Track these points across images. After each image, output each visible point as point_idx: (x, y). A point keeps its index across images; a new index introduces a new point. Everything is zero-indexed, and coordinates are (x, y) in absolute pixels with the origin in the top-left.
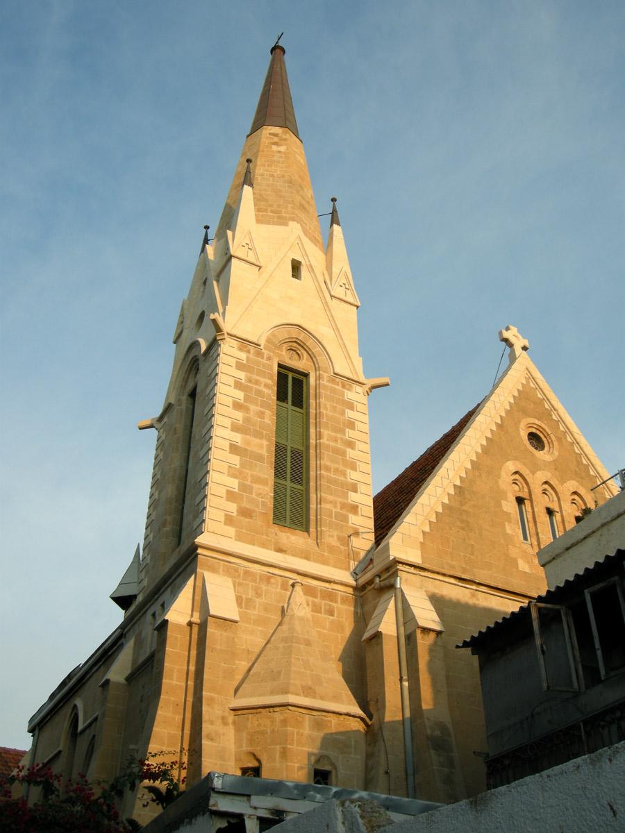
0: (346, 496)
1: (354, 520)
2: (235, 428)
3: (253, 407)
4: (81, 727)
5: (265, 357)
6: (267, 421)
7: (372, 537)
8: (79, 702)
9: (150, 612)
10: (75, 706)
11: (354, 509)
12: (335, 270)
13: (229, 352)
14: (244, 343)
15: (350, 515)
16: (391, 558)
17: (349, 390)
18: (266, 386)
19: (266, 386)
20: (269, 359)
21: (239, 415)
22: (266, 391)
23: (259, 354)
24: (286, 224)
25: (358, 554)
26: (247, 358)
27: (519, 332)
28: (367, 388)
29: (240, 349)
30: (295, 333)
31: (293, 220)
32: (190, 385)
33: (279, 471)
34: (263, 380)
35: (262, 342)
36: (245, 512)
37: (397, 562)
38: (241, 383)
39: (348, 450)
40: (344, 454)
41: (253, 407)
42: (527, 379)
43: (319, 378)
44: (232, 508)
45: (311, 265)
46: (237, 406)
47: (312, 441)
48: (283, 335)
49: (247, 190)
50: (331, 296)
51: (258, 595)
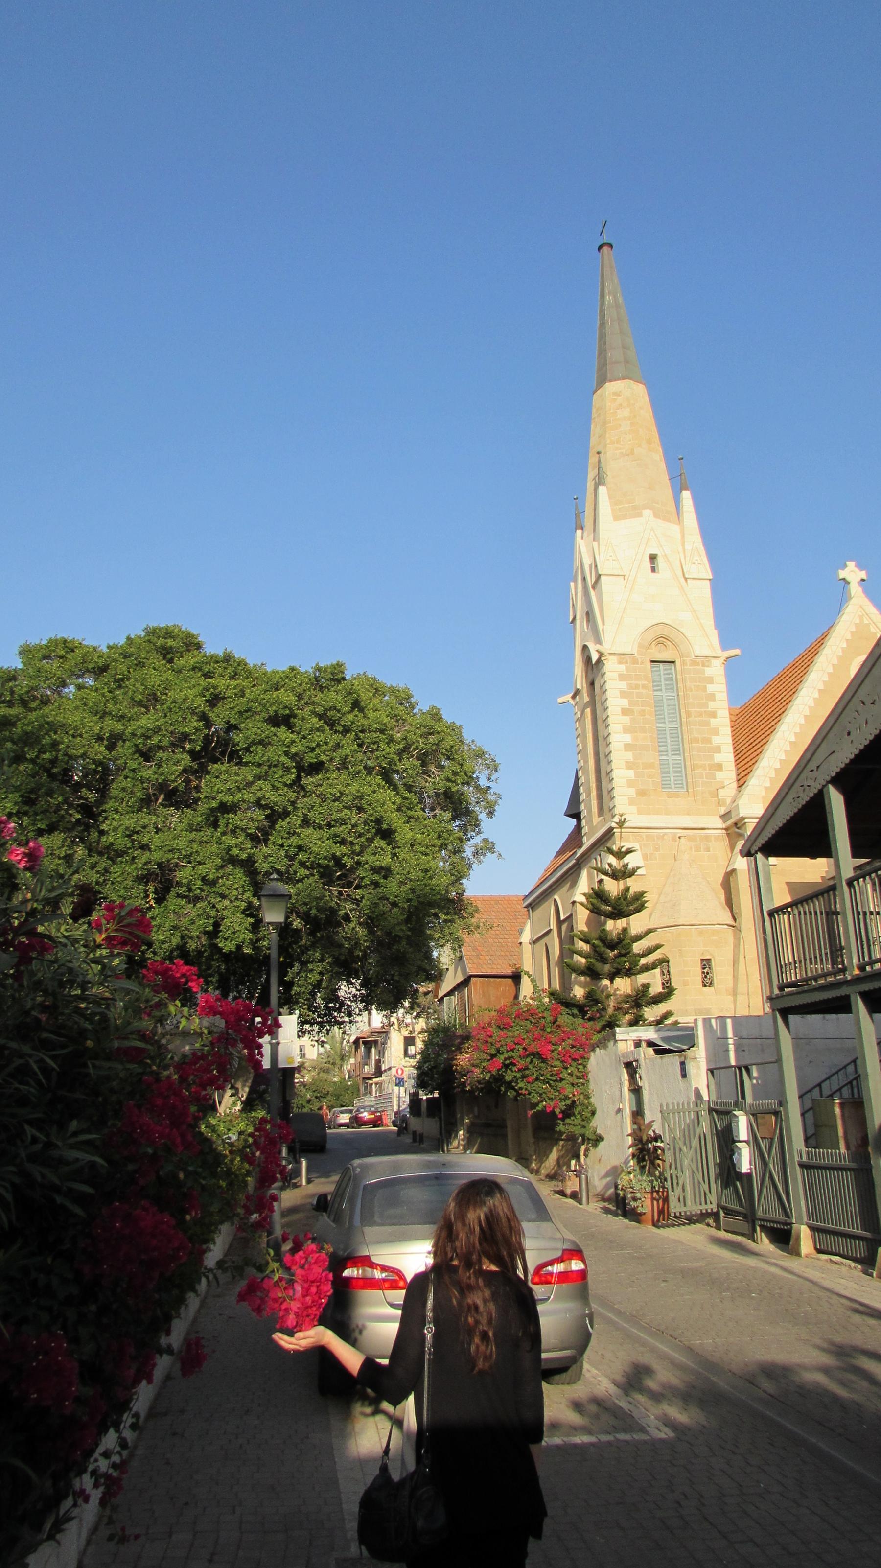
0: (712, 757)
1: (719, 775)
2: (626, 730)
3: (636, 709)
4: (562, 918)
5: (640, 661)
6: (647, 716)
7: (735, 785)
8: (556, 897)
9: (593, 856)
10: (555, 900)
11: (719, 767)
12: (688, 547)
13: (612, 670)
14: (622, 657)
15: (717, 773)
16: (741, 815)
17: (708, 666)
18: (644, 687)
19: (644, 687)
20: (642, 663)
21: (626, 719)
22: (644, 691)
23: (635, 661)
24: (640, 515)
25: (724, 801)
26: (626, 668)
27: (856, 566)
28: (722, 660)
29: (620, 663)
30: (659, 631)
31: (646, 507)
32: (590, 680)
33: (662, 749)
34: (640, 683)
35: (635, 652)
36: (642, 793)
37: (743, 818)
38: (624, 692)
39: (712, 720)
40: (708, 724)
41: (636, 709)
42: (861, 617)
43: (683, 663)
44: (632, 792)
45: (665, 555)
46: (625, 712)
47: (684, 720)
48: (651, 636)
49: (602, 489)
50: (686, 579)
51: (657, 849)
